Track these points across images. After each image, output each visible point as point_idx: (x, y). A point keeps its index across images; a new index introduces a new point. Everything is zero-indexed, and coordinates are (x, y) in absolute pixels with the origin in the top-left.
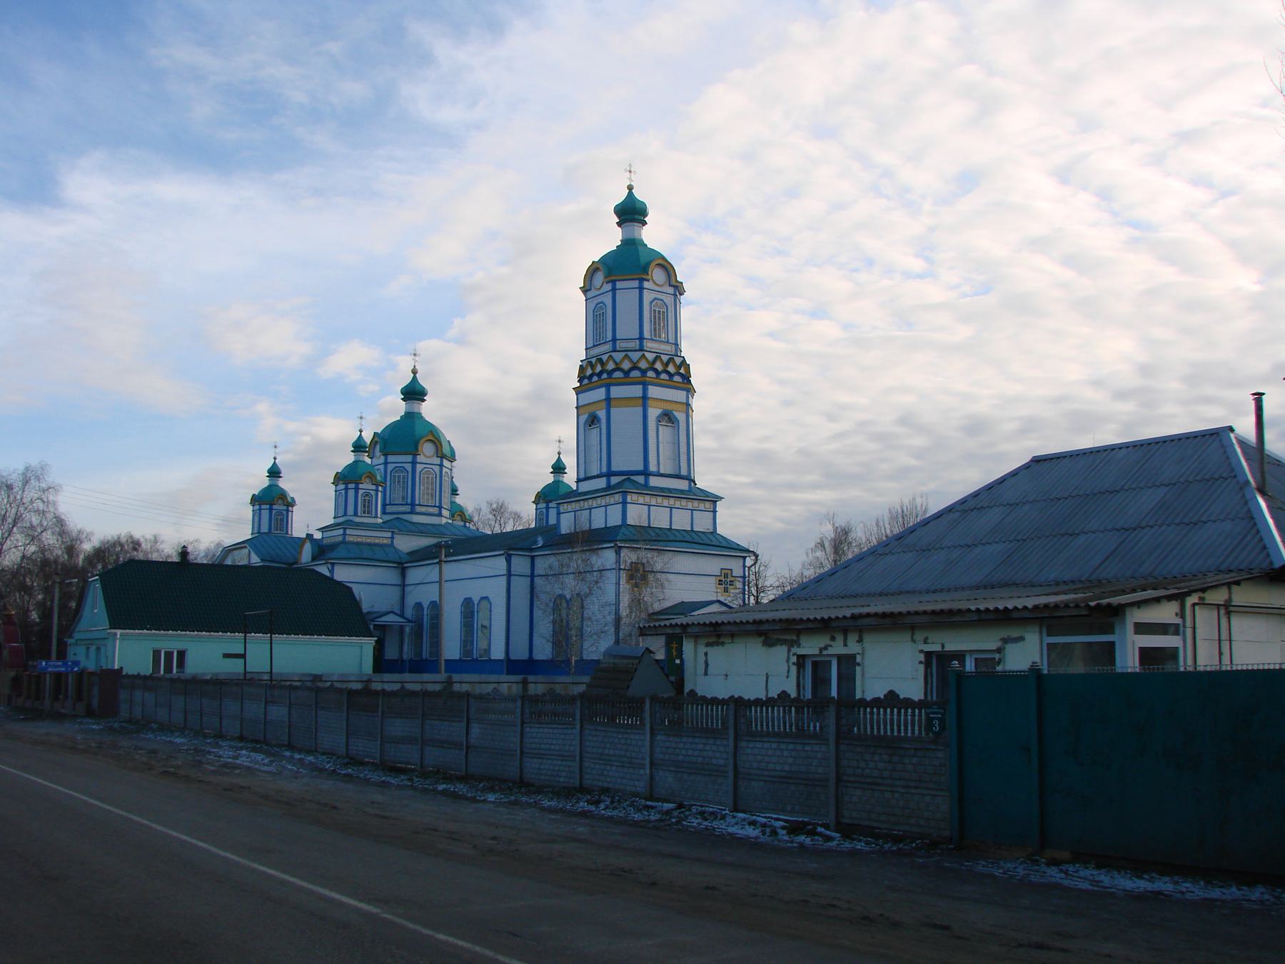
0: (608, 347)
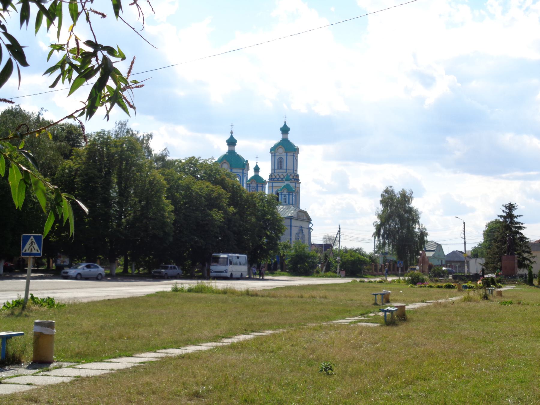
0: (285, 171)
